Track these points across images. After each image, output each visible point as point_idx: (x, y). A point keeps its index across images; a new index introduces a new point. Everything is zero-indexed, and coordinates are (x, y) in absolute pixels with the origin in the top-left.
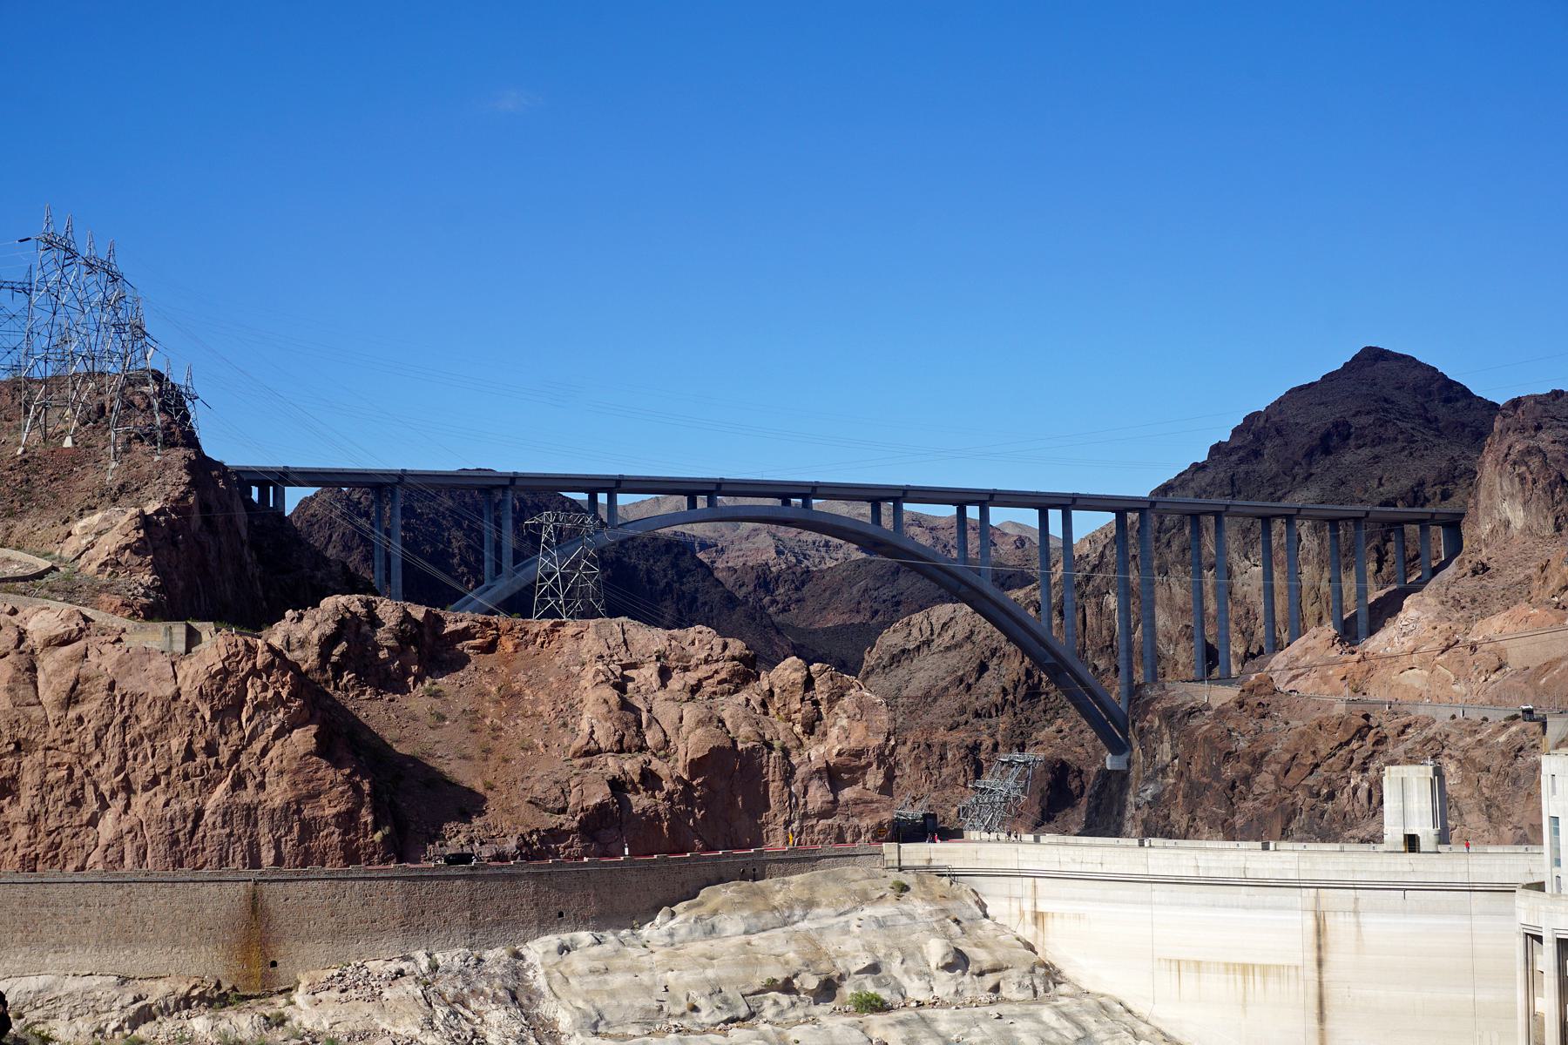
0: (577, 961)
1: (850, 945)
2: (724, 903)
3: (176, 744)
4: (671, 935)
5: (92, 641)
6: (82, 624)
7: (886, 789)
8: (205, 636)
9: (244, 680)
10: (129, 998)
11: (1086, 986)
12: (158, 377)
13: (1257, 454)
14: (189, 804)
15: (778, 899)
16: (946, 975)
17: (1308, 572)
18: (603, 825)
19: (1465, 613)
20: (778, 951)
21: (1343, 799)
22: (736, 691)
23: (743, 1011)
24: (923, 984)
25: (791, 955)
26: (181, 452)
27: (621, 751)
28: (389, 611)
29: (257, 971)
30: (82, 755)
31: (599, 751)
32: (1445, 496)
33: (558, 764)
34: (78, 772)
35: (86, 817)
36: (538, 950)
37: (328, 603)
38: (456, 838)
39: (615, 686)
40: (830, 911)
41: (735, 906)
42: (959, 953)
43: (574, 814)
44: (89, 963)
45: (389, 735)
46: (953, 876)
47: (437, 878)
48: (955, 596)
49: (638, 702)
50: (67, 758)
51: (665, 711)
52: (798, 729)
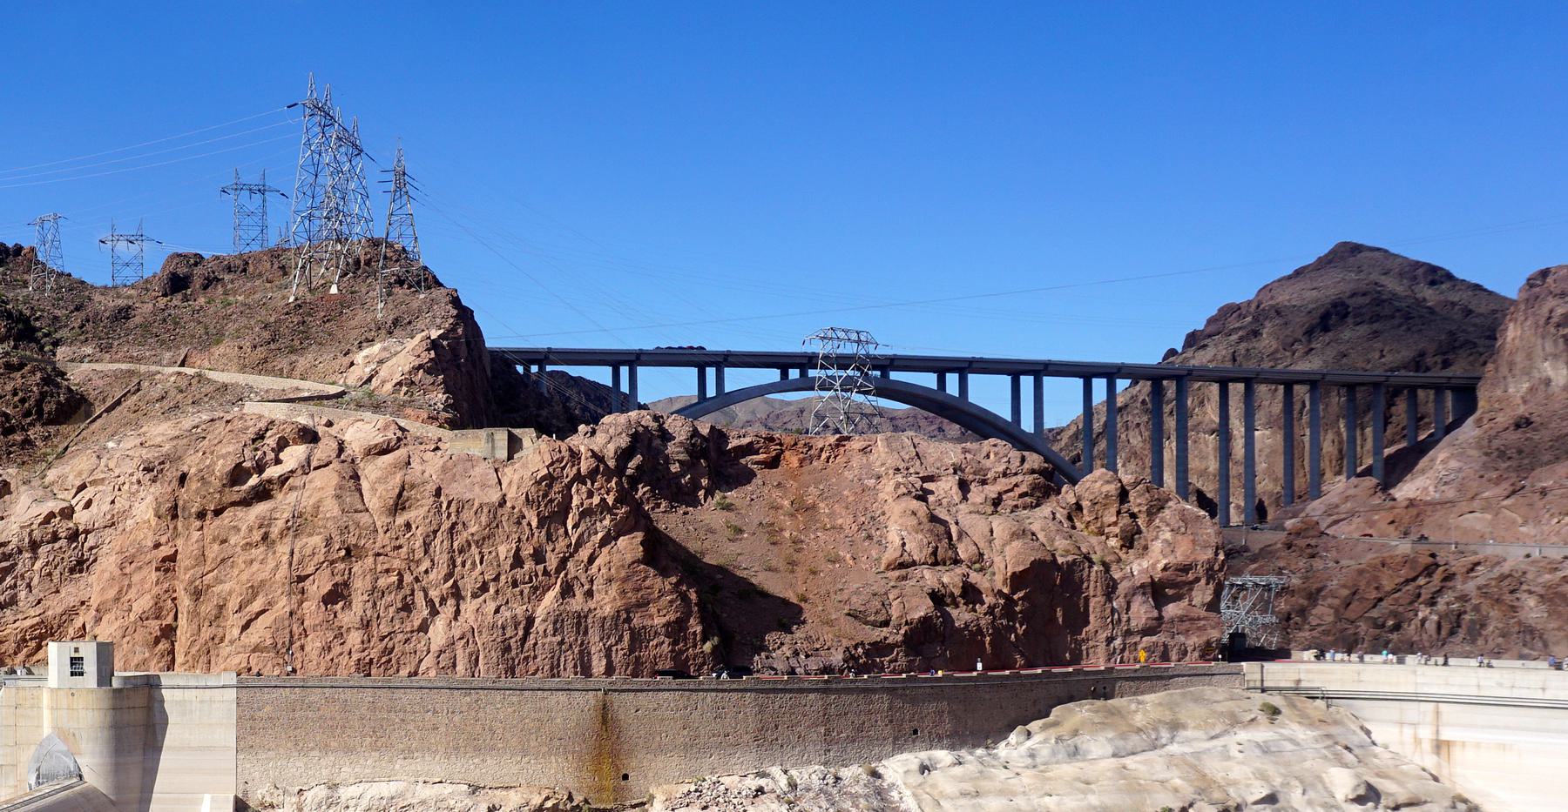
1: (1238, 772)
2: (1083, 723)
3: (504, 550)
6: (399, 434)
8: (526, 443)
9: (569, 486)
15: (1139, 720)
18: (929, 639)
20: (1162, 776)
22: (1038, 505)
25: (1178, 782)
27: (936, 564)
31: (914, 563)
33: (871, 577)
35: (417, 623)
36: (898, 768)
38: (780, 650)
39: (918, 498)
40: (1200, 734)
42: (1370, 787)
43: (899, 627)
45: (693, 546)
47: (790, 691)
49: (943, 515)
51: (967, 520)
52: (1113, 542)
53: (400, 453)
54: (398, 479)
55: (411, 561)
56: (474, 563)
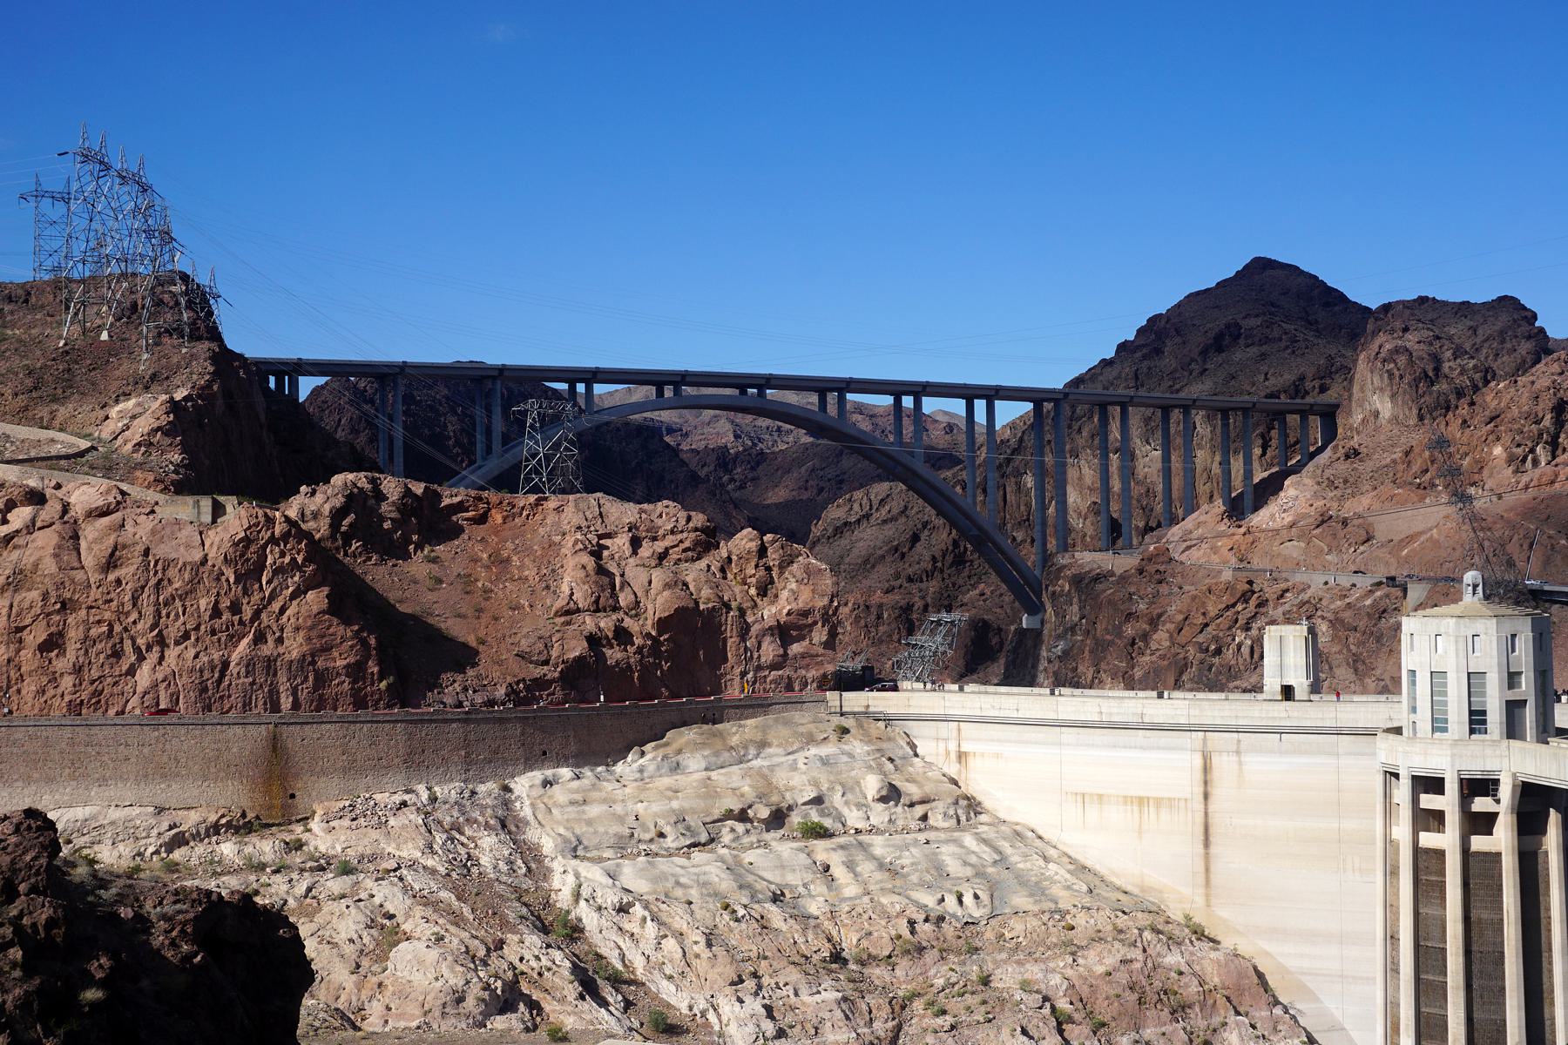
0: (559, 794)
1: (797, 780)
2: (687, 743)
3: (204, 603)
4: (641, 771)
5: (129, 513)
6: (119, 498)
7: (830, 644)
8: (229, 509)
9: (264, 547)
10: (165, 826)
11: (1002, 815)
12: (185, 278)
13: (1158, 352)
14: (216, 656)
15: (735, 740)
16: (881, 806)
17: (1201, 456)
18: (582, 676)
19: (1338, 493)
20: (734, 785)
21: (1229, 654)
22: (699, 558)
23: (703, 838)
24: (861, 814)
25: (746, 789)
26: (206, 345)
27: (597, 610)
28: (392, 487)
29: (278, 802)
30: (121, 613)
31: (578, 610)
32: (1323, 389)
34: (117, 628)
35: (125, 668)
36: (524, 785)
37: (338, 479)
38: (452, 687)
39: (592, 553)
40: (780, 751)
41: (696, 746)
42: (892, 787)
43: (557, 665)
44: (129, 795)
45: (392, 596)
46: (888, 720)
47: (435, 721)
48: (890, 476)
50: (107, 615)
51: (636, 574)
52: (753, 591)
53: (117, 516)
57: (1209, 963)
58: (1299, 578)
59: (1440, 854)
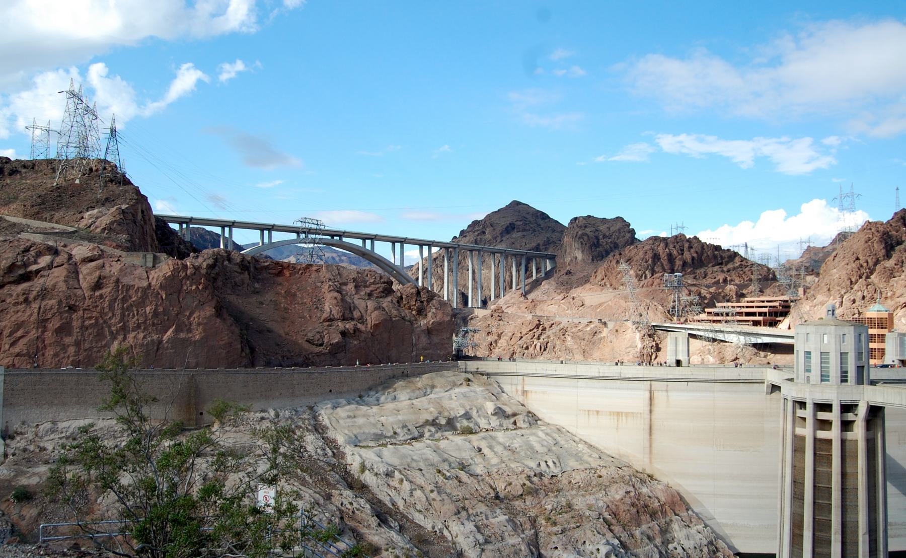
13: (484, 233)
15: (419, 385)
16: (495, 418)
20: (426, 407)
21: (531, 349)
23: (416, 434)
24: (486, 421)
25: (432, 409)
32: (546, 250)
40: (442, 390)
46: (489, 375)
52: (414, 312)
54: (97, 273)
55: (102, 313)
56: (134, 315)
57: (659, 491)
58: (557, 319)
59: (829, 442)
